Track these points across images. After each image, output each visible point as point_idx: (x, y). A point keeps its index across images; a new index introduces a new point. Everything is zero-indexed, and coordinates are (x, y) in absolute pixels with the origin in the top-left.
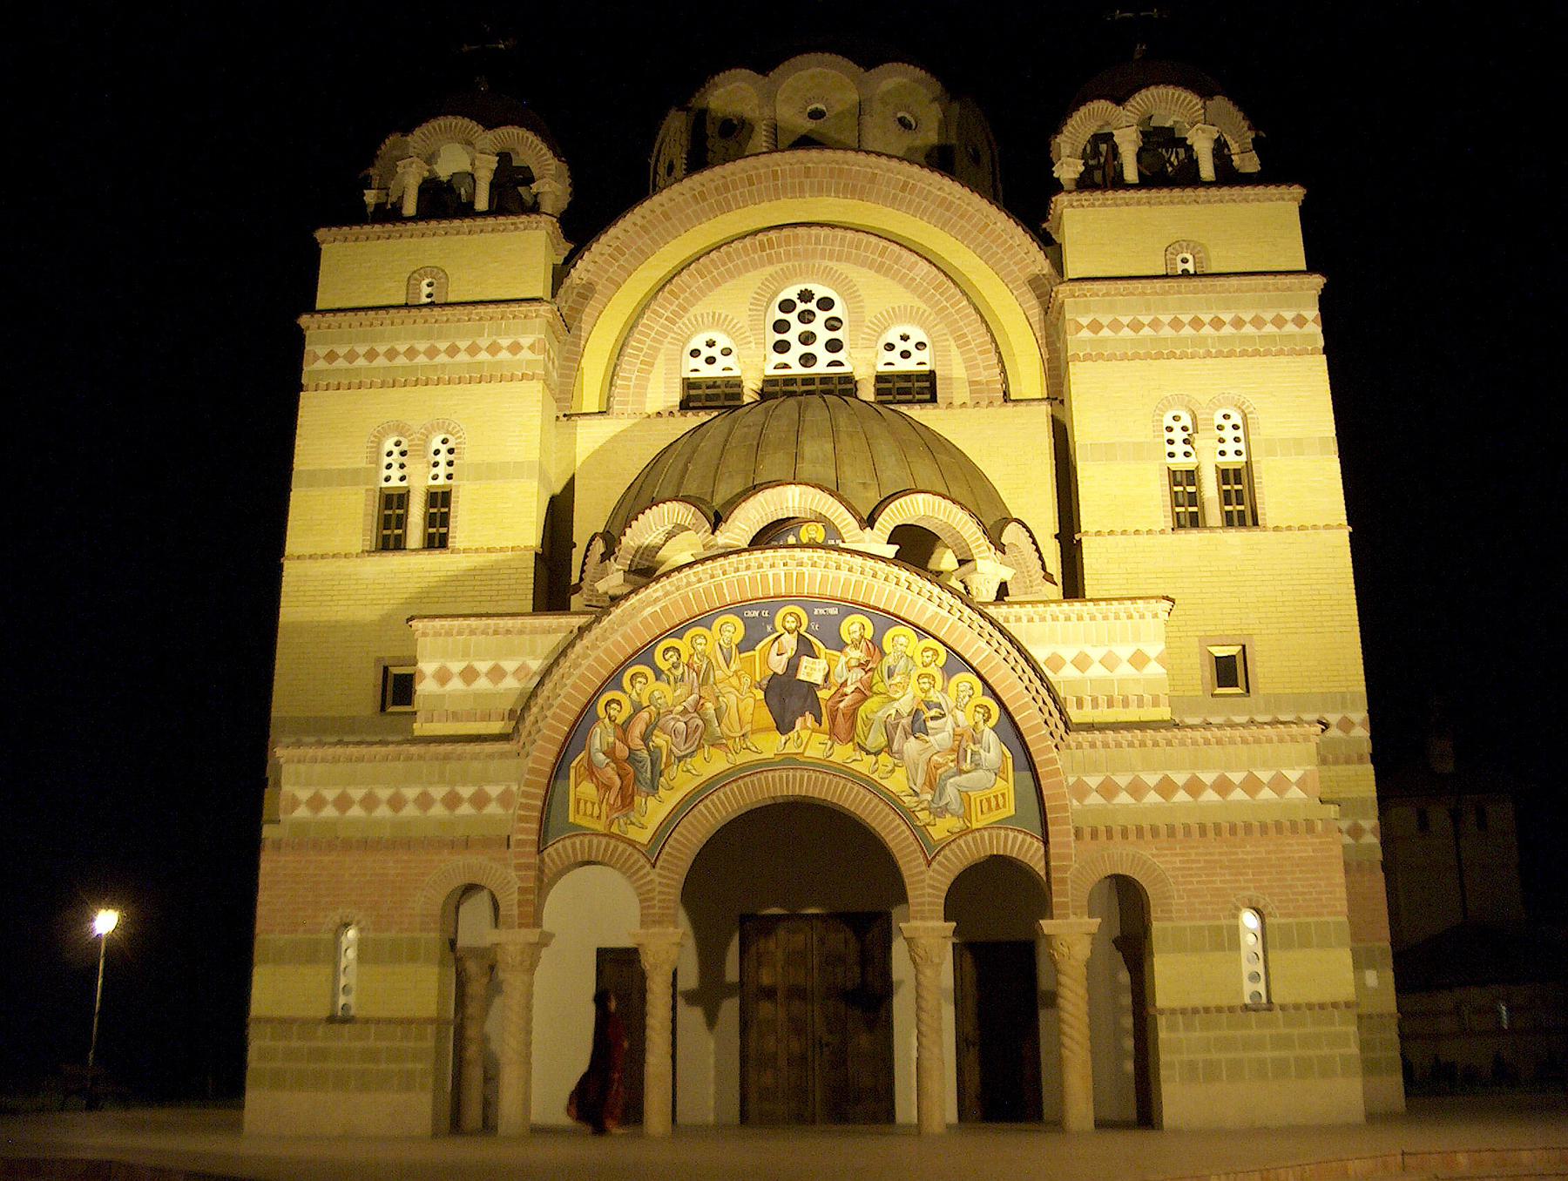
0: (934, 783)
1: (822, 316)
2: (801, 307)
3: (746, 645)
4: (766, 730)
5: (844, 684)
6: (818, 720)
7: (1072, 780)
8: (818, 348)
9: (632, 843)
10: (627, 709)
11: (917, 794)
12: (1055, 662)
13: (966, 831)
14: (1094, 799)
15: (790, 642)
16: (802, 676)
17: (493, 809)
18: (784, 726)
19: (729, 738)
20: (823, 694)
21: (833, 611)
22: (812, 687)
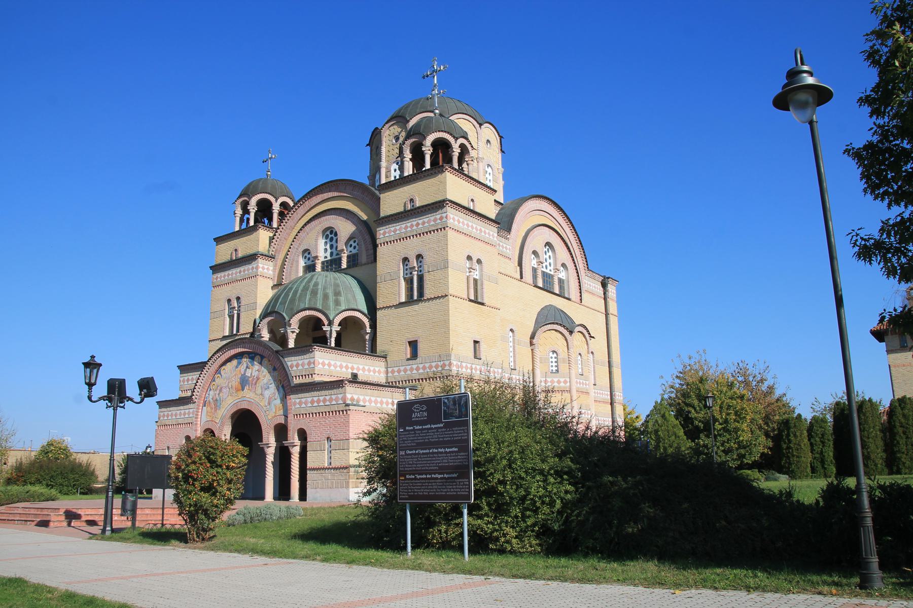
0: (269, 404)
1: (335, 238)
2: (330, 236)
3: (237, 367)
4: (239, 390)
5: (254, 376)
6: (249, 387)
7: (293, 400)
8: (334, 250)
9: (216, 422)
10: (216, 387)
11: (266, 406)
12: (292, 366)
13: (275, 416)
14: (298, 406)
15: (245, 365)
16: (247, 375)
17: (191, 416)
18: (243, 390)
19: (233, 393)
20: (250, 379)
21: (253, 355)
22: (248, 377)
